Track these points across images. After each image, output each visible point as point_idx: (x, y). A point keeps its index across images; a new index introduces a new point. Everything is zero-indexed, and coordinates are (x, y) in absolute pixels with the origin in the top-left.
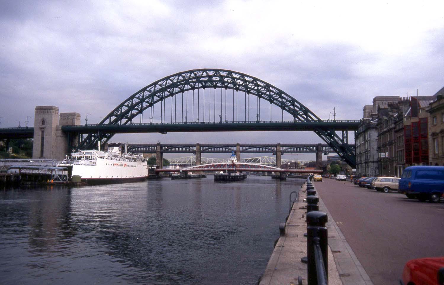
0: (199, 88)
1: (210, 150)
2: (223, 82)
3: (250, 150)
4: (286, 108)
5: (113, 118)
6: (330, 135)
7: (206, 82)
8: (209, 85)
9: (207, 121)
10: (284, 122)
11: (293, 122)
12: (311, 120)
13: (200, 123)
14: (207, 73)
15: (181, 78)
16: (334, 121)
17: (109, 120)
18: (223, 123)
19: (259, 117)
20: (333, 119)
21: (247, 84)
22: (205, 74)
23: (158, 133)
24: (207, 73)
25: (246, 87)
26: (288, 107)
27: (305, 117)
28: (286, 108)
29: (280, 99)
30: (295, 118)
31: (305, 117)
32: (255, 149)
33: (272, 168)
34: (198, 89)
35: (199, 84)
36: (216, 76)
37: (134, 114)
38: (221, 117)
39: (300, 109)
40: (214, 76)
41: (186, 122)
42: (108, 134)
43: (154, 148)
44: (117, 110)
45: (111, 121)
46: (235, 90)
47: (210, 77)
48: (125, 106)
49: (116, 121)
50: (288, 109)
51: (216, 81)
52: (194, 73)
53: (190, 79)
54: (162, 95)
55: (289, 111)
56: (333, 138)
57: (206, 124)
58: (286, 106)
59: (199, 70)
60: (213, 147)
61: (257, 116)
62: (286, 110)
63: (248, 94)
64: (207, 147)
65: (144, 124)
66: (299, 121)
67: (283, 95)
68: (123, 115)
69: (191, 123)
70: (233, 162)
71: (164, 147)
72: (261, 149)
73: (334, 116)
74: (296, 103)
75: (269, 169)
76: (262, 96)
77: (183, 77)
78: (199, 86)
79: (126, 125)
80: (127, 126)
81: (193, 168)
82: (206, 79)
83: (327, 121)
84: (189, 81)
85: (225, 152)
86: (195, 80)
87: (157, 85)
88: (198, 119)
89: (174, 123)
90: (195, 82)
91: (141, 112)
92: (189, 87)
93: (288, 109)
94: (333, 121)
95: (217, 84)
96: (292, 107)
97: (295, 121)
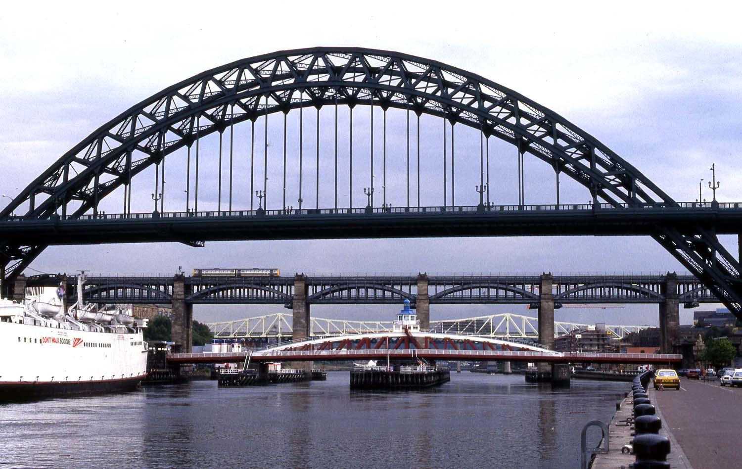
0: (302, 104)
1: (336, 294)
2: (376, 89)
3: (458, 294)
4: (567, 165)
5: (41, 198)
6: (700, 247)
7: (324, 87)
8: (333, 96)
9: (326, 205)
10: (561, 208)
11: (590, 208)
12: (643, 201)
13: (306, 212)
14: (326, 61)
15: (248, 76)
16: (715, 203)
17: (27, 202)
18: (375, 211)
19: (485, 194)
20: (712, 200)
21: (449, 93)
22: (321, 63)
24: (326, 61)
25: (446, 101)
27: (626, 192)
28: (567, 165)
29: (549, 140)
30: (594, 196)
31: (626, 192)
32: (475, 292)
33: (527, 350)
34: (300, 109)
36: (354, 70)
37: (104, 184)
38: (369, 195)
39: (611, 170)
40: (349, 68)
41: (263, 208)
42: (25, 249)
43: (166, 289)
44: (52, 172)
46: (412, 113)
47: (337, 72)
48: (79, 161)
49: (49, 206)
50: (573, 169)
51: (353, 85)
52: (287, 61)
53: (275, 77)
54: (192, 128)
55: (578, 175)
56: (711, 257)
57: (325, 215)
58: (569, 160)
59: (303, 52)
60: (345, 286)
61: (479, 189)
62: (568, 171)
63: (453, 123)
64: (328, 285)
65: (134, 217)
66: (609, 206)
67: (559, 127)
69: (279, 211)
70: (406, 332)
71: (195, 288)
72: (493, 292)
73: (714, 188)
74: (597, 152)
75: (519, 354)
76: (496, 128)
77: (255, 72)
78: (301, 99)
79: (81, 218)
80: (84, 221)
81: (286, 349)
82: (325, 78)
83: (693, 204)
84: (274, 84)
85: (383, 301)
86: (291, 81)
87: (175, 98)
88: (300, 201)
89: (228, 214)
90: (291, 88)
91: (125, 178)
92: (272, 102)
93: (573, 169)
94: (709, 205)
95: (357, 92)
96: (585, 163)
97: (596, 205)
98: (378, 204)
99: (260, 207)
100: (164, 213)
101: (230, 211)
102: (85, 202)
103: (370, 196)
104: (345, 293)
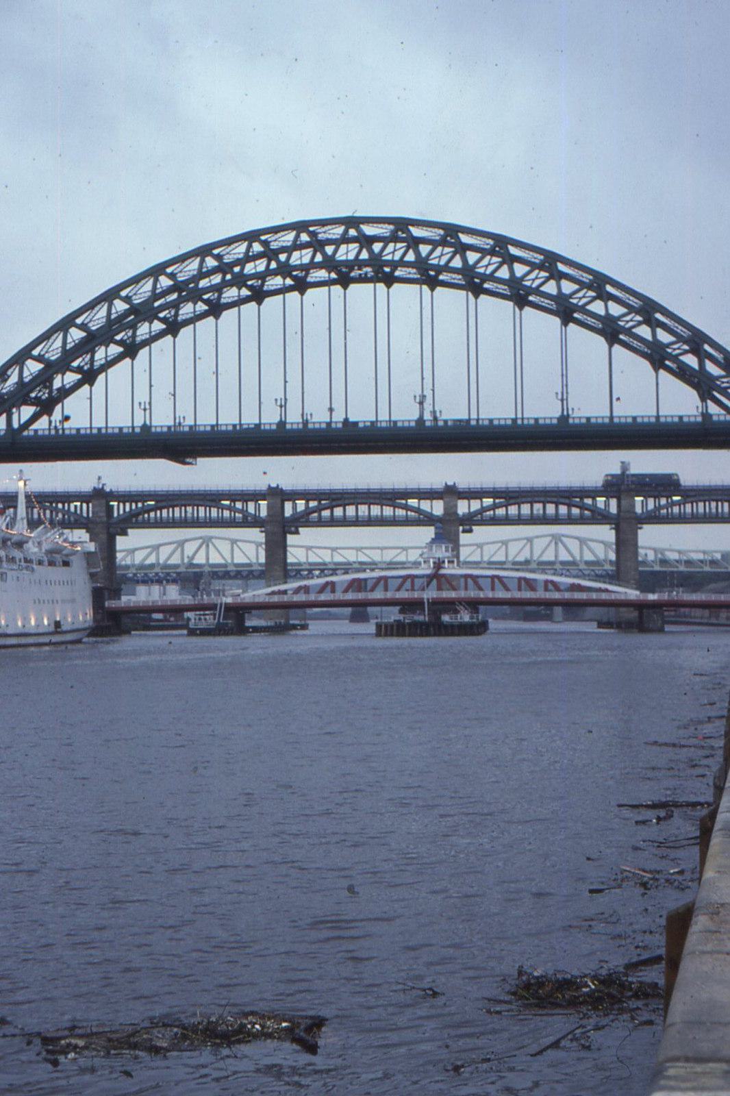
3: (501, 512)
33: (607, 591)
75: (594, 596)
79: (25, 433)
85: (406, 522)
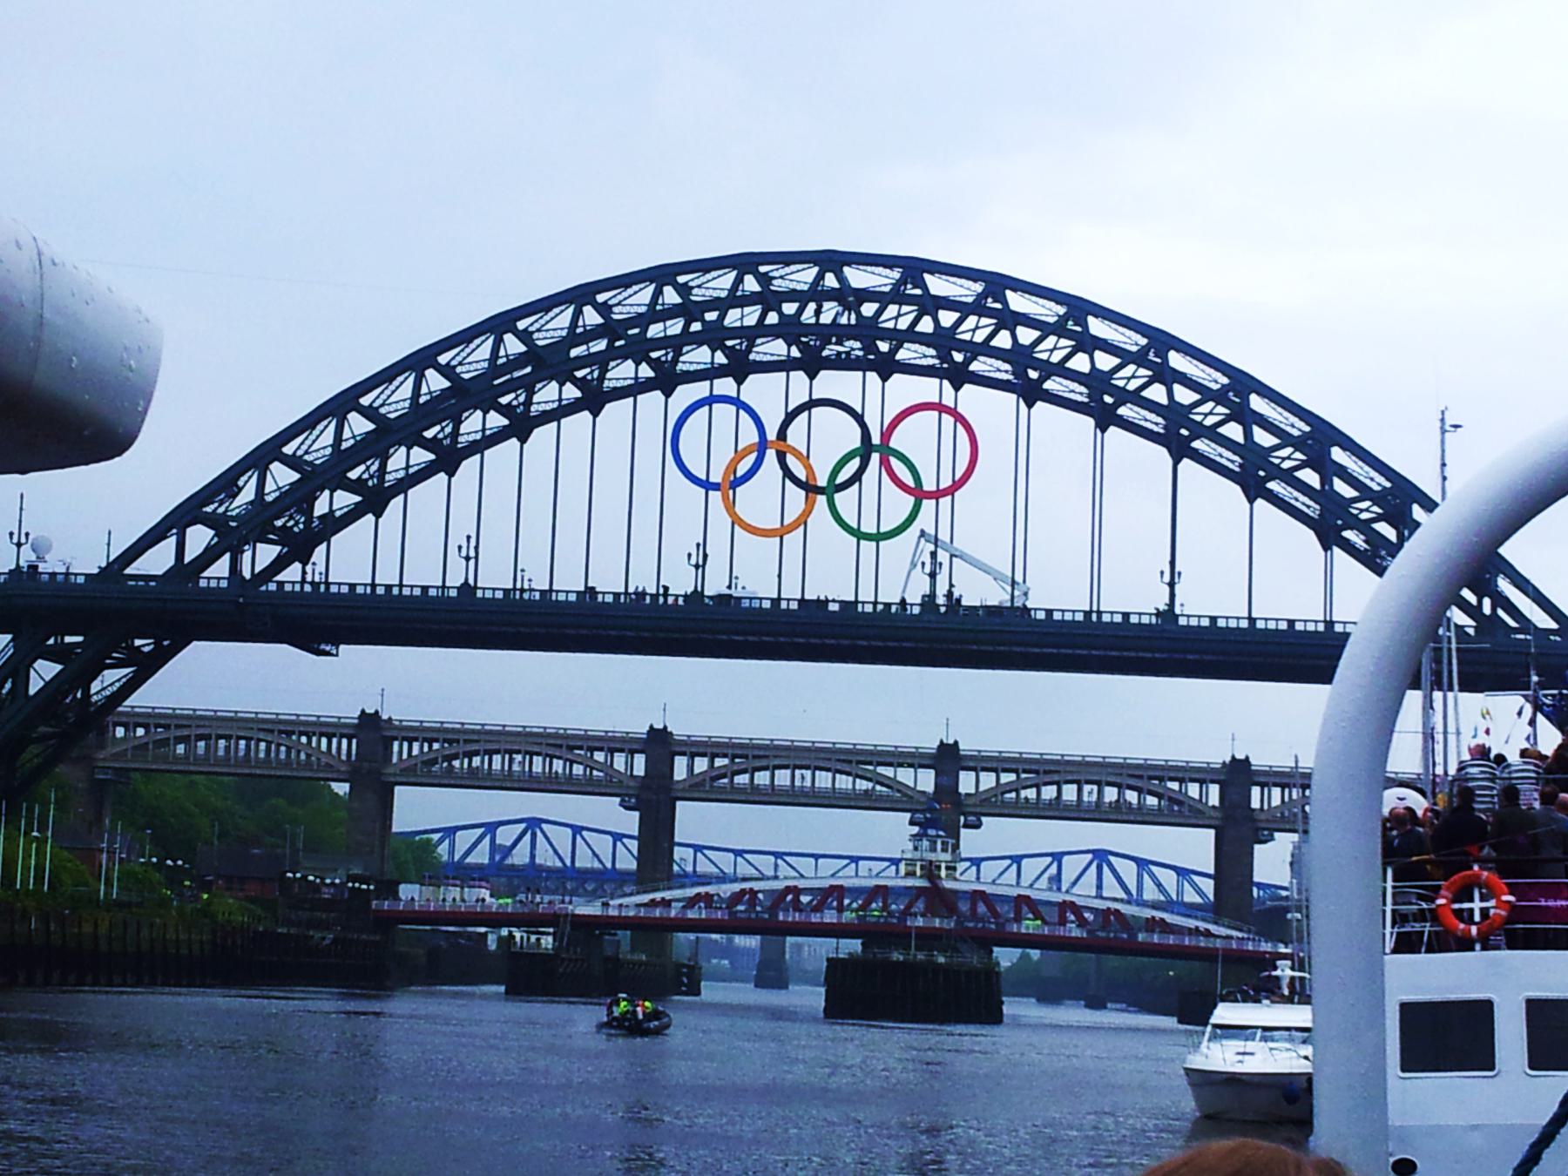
1: (742, 779)
4: (1348, 534)
12: (1513, 624)
22: (751, 284)
23: (285, 646)
26: (1365, 527)
28: (1348, 534)
35: (713, 352)
38: (697, 566)
45: (187, 559)
60: (764, 763)
61: (1167, 578)
68: (258, 523)
69: (617, 595)
89: (395, 591)
98: (791, 591)
99: (467, 579)
100: (448, 588)
101: (401, 586)
102: (285, 550)
103: (700, 570)
104: (762, 778)
